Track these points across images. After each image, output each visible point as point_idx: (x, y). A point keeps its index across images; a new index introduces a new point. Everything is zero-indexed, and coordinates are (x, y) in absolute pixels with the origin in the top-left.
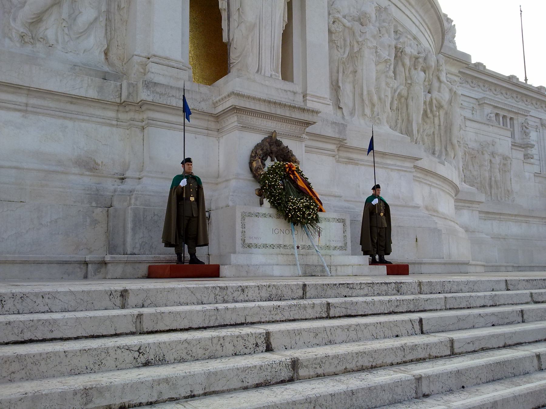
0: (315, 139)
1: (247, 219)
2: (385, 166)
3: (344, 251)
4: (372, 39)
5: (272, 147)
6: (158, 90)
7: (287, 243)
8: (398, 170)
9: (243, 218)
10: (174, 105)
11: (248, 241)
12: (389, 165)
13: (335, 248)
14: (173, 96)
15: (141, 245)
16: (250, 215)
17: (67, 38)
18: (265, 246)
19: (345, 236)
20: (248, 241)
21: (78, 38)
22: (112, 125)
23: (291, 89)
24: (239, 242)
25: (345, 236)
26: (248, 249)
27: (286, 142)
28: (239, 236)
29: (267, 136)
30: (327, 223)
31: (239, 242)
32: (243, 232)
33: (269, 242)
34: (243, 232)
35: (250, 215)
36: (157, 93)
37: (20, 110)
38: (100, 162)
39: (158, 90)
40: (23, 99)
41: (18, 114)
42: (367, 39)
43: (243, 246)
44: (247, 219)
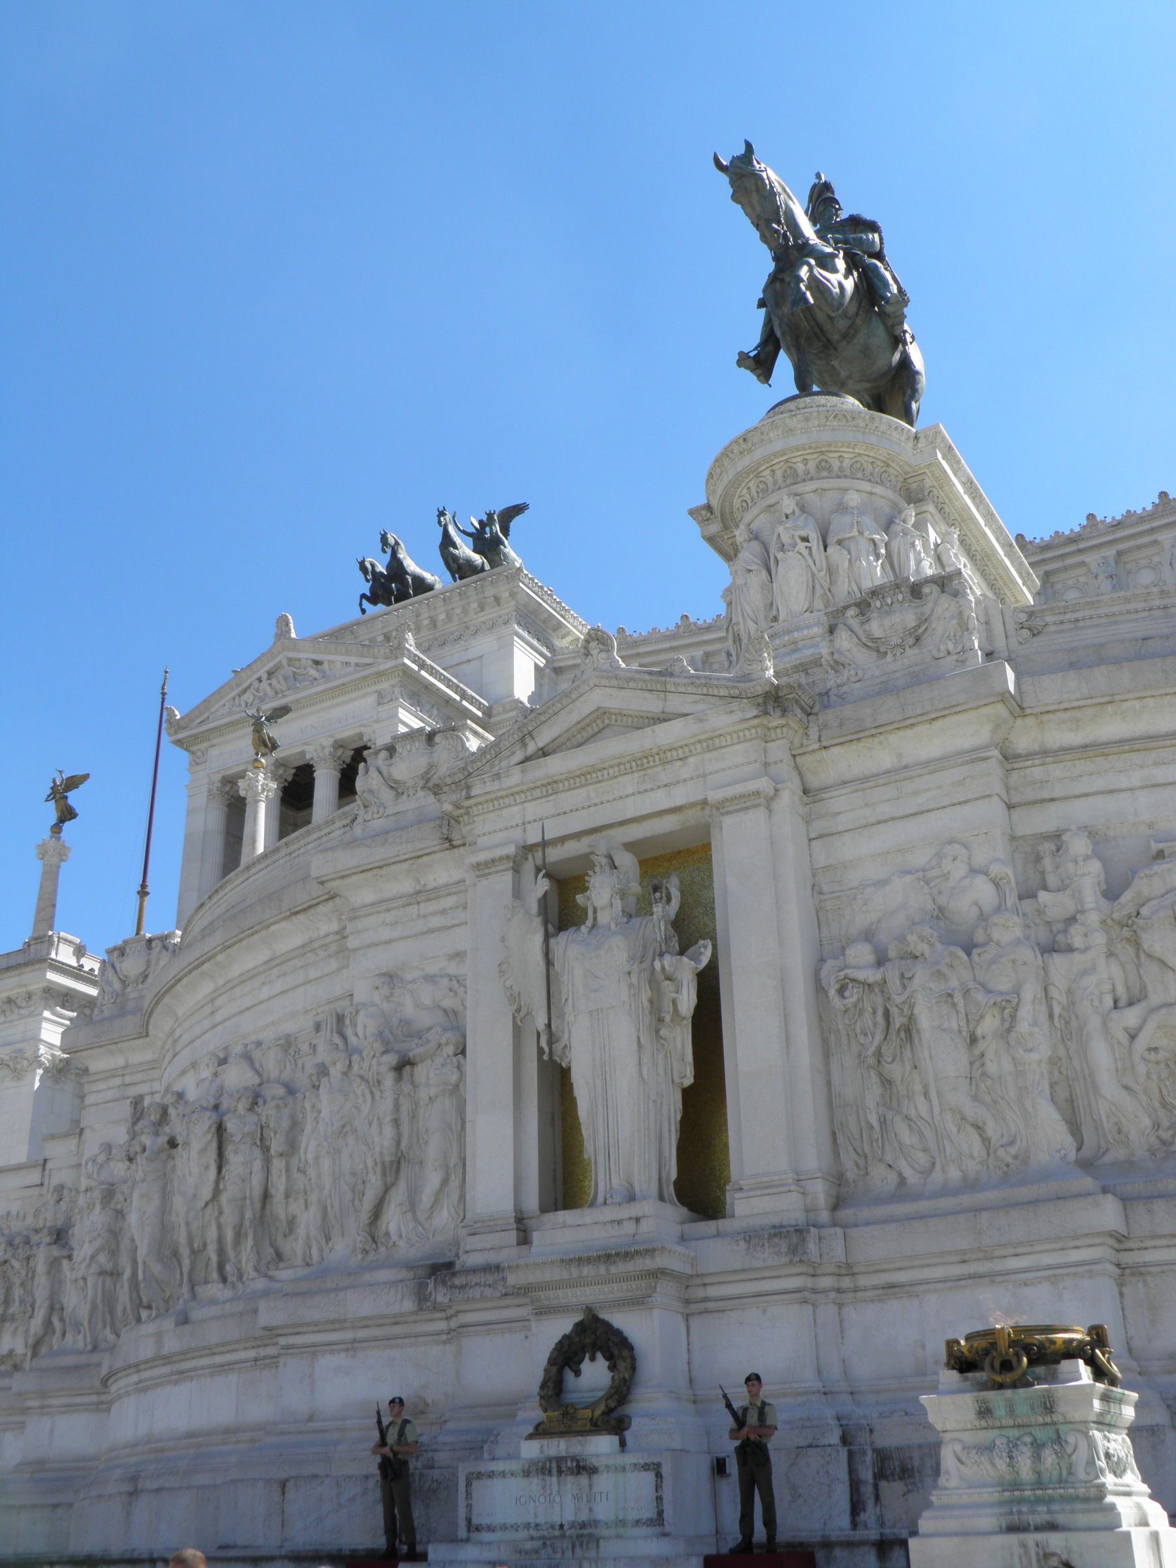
1: (475, 1483)
3: (658, 1529)
5: (594, 1337)
9: (469, 1484)
11: (475, 1521)
13: (637, 1523)
14: (476, 1284)
16: (479, 1476)
18: (504, 1527)
19: (659, 1499)
22: (444, 1342)
23: (634, 1214)
24: (462, 1524)
25: (659, 1499)
27: (620, 1320)
28: (462, 1512)
33: (511, 1520)
35: (479, 1476)
36: (456, 1287)
37: (347, 1350)
38: (430, 1401)
39: (457, 1281)
40: (349, 1335)
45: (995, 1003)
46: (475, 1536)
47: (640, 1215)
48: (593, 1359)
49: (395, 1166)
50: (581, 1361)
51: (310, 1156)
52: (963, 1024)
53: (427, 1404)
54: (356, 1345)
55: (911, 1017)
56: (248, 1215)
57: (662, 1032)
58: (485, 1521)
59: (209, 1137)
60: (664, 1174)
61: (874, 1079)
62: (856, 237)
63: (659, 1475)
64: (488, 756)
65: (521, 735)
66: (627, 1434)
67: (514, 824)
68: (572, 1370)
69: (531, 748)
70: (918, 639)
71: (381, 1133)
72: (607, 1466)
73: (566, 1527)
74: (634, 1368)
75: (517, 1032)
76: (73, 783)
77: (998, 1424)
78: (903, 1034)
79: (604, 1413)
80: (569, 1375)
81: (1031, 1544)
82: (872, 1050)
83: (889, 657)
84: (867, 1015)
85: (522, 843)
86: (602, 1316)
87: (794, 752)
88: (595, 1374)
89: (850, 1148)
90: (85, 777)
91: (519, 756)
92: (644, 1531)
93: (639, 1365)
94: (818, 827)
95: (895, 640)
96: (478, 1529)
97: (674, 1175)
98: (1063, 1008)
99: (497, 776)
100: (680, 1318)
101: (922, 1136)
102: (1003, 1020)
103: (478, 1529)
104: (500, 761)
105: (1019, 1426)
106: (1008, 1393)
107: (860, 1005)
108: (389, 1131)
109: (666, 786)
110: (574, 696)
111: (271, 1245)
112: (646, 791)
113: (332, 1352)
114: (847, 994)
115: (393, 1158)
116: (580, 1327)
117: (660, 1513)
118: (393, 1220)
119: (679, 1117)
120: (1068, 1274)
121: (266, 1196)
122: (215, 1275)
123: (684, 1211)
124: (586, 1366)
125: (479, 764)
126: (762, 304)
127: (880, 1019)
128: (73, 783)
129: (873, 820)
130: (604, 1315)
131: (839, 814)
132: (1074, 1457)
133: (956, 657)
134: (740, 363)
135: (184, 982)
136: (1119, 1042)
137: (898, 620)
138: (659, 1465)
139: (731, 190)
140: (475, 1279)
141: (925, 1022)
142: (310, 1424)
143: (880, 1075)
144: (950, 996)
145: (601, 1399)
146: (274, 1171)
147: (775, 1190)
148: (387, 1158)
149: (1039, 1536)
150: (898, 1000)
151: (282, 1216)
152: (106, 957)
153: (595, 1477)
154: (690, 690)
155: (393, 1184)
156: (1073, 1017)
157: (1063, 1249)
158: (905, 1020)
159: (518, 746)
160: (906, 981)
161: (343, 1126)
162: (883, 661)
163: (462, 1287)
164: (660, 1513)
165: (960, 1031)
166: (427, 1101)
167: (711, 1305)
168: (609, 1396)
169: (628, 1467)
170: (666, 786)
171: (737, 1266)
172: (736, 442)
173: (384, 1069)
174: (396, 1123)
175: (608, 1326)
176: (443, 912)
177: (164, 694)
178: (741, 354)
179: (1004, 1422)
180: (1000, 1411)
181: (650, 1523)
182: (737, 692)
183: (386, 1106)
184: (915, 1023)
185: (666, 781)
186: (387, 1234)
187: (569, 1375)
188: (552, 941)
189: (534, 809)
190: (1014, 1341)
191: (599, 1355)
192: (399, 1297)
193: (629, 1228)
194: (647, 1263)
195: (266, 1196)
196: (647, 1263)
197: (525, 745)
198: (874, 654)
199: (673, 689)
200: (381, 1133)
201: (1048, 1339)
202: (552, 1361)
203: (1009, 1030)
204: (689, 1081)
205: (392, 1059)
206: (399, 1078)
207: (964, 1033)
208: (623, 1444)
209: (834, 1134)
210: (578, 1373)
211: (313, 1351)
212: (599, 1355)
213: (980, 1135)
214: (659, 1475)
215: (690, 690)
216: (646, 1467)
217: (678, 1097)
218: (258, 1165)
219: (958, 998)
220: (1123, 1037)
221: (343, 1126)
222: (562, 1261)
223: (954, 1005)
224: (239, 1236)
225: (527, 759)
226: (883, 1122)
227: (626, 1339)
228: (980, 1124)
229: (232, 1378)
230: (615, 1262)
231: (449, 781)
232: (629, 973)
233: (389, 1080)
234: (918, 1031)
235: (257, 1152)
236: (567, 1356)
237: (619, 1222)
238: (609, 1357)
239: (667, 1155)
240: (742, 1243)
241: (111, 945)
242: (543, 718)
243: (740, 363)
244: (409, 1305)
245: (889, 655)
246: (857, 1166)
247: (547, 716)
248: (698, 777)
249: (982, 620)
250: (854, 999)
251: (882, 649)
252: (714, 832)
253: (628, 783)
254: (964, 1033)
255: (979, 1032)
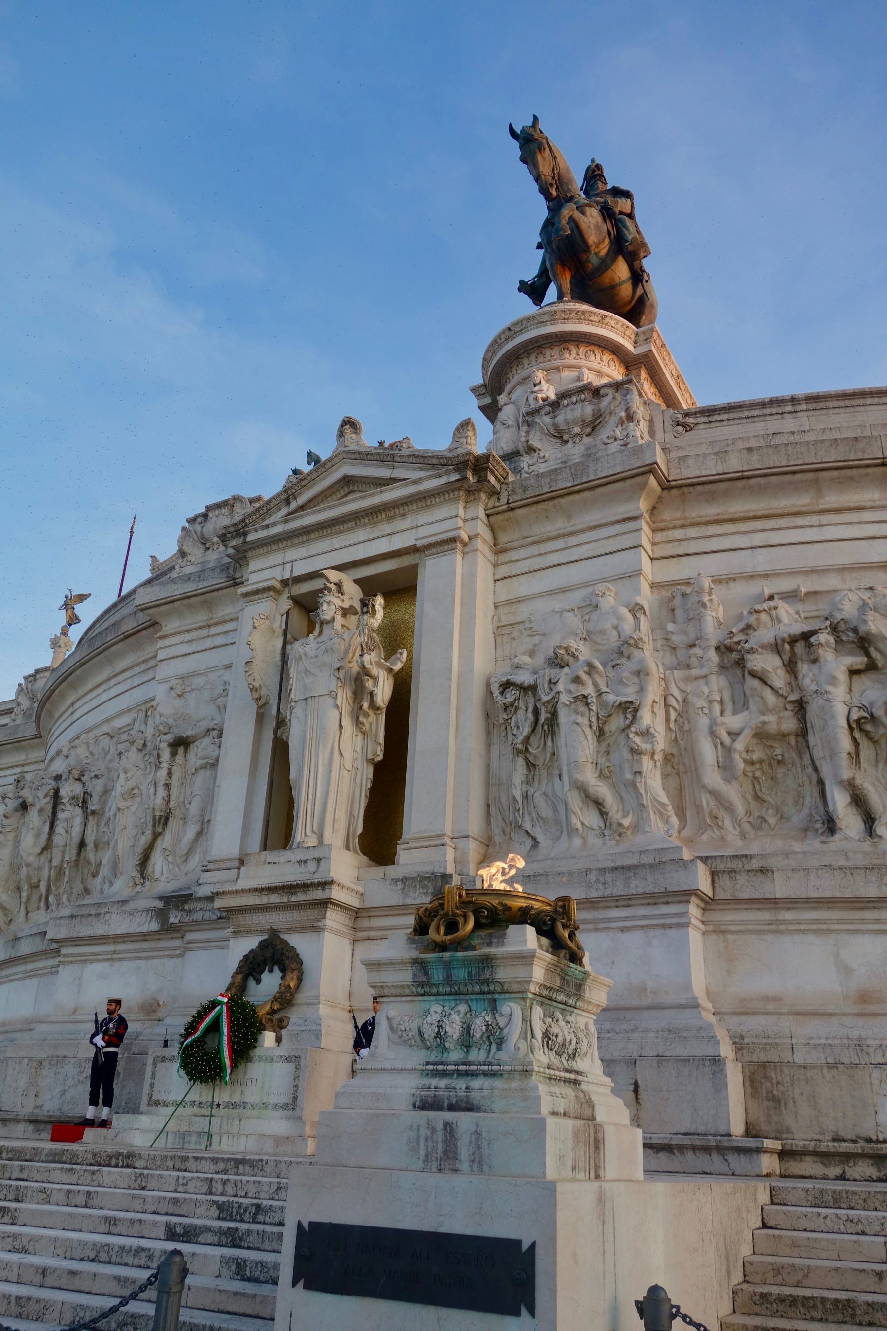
0: (401, 912)
1: (159, 1065)
2: (602, 926)
4: (572, 687)
6: (186, 907)
7: (204, 1099)
8: (642, 927)
10: (200, 919)
11: (155, 1097)
12: (610, 920)
13: (276, 1106)
15: (126, 1103)
17: (171, 866)
20: (155, 1097)
21: (186, 861)
23: (317, 856)
24: (145, 1099)
26: (154, 1108)
28: (146, 1087)
29: (266, 937)
30: (268, 1065)
31: (145, 1099)
32: (152, 1085)
34: (152, 1085)
37: (108, 960)
38: (161, 1003)
40: (111, 948)
41: (107, 964)
42: (558, 693)
43: (149, 1104)
44: (159, 1065)
45: (620, 704)
46: (154, 1108)
47: (322, 856)
48: (271, 971)
49: (163, 820)
50: (262, 972)
51: (112, 813)
52: (594, 719)
53: (159, 1005)
54: (115, 956)
55: (554, 714)
56: (67, 858)
57: (361, 719)
58: (162, 1097)
59: (49, 798)
60: (351, 830)
61: (521, 761)
62: (614, 206)
63: (298, 1068)
64: (261, 512)
65: (286, 496)
66: (284, 1032)
67: (276, 563)
68: (254, 978)
69: (294, 505)
70: (594, 429)
71: (155, 794)
72: (259, 1057)
73: (221, 1107)
74: (300, 980)
75: (260, 718)
76: (82, 598)
77: (434, 990)
78: (546, 727)
79: (268, 1013)
80: (252, 983)
81: (440, 1126)
82: (521, 738)
83: (570, 444)
84: (521, 713)
85: (280, 578)
86: (282, 936)
87: (488, 512)
88: (270, 982)
89: (500, 818)
90: (89, 595)
91: (284, 511)
92: (281, 1113)
93: (305, 977)
94: (503, 571)
95: (577, 430)
96: (157, 1103)
97: (360, 830)
98: (679, 714)
99: (267, 527)
100: (347, 944)
101: (555, 810)
102: (626, 718)
103: (157, 1103)
104: (270, 516)
105: (456, 994)
106: (447, 955)
107: (516, 704)
108: (161, 792)
109: (389, 535)
110: (327, 467)
111: (82, 882)
112: (374, 539)
113: (98, 961)
114: (508, 695)
115: (163, 814)
116: (263, 945)
117: (295, 1099)
118: (157, 862)
119: (369, 785)
120: (658, 925)
121: (82, 845)
122: (42, 904)
123: (365, 859)
124: (266, 976)
125: (254, 517)
126: (539, 247)
127: (530, 716)
128: (82, 598)
129: (544, 566)
130: (285, 937)
131: (518, 561)
132: (505, 1031)
133: (621, 442)
134: (520, 290)
135: (56, 692)
136: (722, 744)
137: (579, 415)
138: (298, 1058)
139: (520, 153)
140: (200, 905)
141: (564, 717)
142: (72, 1017)
143: (526, 759)
144: (585, 697)
145: (266, 1003)
146: (89, 826)
147: (432, 843)
148: (158, 814)
149: (449, 1116)
150: (545, 698)
151: (92, 860)
152: (23, 682)
153: (250, 1065)
154: (411, 460)
155: (160, 834)
156: (686, 722)
157: (655, 904)
158: (549, 715)
159: (284, 503)
160: (552, 686)
161: (133, 789)
162: (565, 447)
163: (190, 911)
164: (295, 1099)
165: (591, 726)
166: (193, 771)
167: (372, 934)
168: (276, 999)
169: (275, 1058)
170: (389, 535)
171: (393, 902)
172: (504, 332)
173: (164, 745)
174: (167, 786)
175: (286, 943)
176: (226, 633)
177: (132, 532)
178: (522, 282)
179: (440, 989)
180: (438, 975)
181: (285, 1107)
182: (445, 461)
183: (163, 773)
184: (557, 719)
185: (389, 531)
186: (153, 872)
187: (252, 983)
188: (288, 647)
189: (292, 554)
190: (464, 903)
191: (276, 968)
192: (149, 919)
193: (312, 866)
194: (319, 894)
195: (82, 845)
196: (319, 894)
197: (288, 503)
198: (559, 441)
199: (399, 460)
200: (155, 794)
201: (501, 903)
202: (240, 969)
203: (629, 726)
204: (380, 758)
205: (169, 738)
206: (174, 754)
207: (594, 728)
208: (279, 1040)
209: (488, 805)
210: (258, 981)
211: (84, 960)
212: (276, 968)
213: (600, 811)
214: (298, 1068)
215: (411, 460)
216: (288, 1059)
217: (371, 770)
218: (78, 821)
219: (593, 699)
220: (727, 739)
221: (133, 789)
222: (256, 890)
223: (588, 704)
224: (60, 872)
225: (289, 514)
226: (526, 796)
227: (298, 955)
228: (601, 801)
229: (34, 981)
230: (295, 893)
231: (231, 530)
232: (338, 669)
233: (166, 755)
234: (558, 725)
235: (78, 811)
236: (252, 967)
237: (306, 861)
238: (283, 970)
239: (356, 814)
240: (399, 883)
241: (26, 674)
242: (303, 483)
243: (520, 290)
244: (154, 926)
245: (570, 442)
246: (504, 832)
247: (307, 481)
248: (413, 528)
249: (648, 418)
250: (512, 700)
251: (565, 437)
252: (420, 570)
253: (361, 534)
254: (594, 728)
255: (606, 728)
